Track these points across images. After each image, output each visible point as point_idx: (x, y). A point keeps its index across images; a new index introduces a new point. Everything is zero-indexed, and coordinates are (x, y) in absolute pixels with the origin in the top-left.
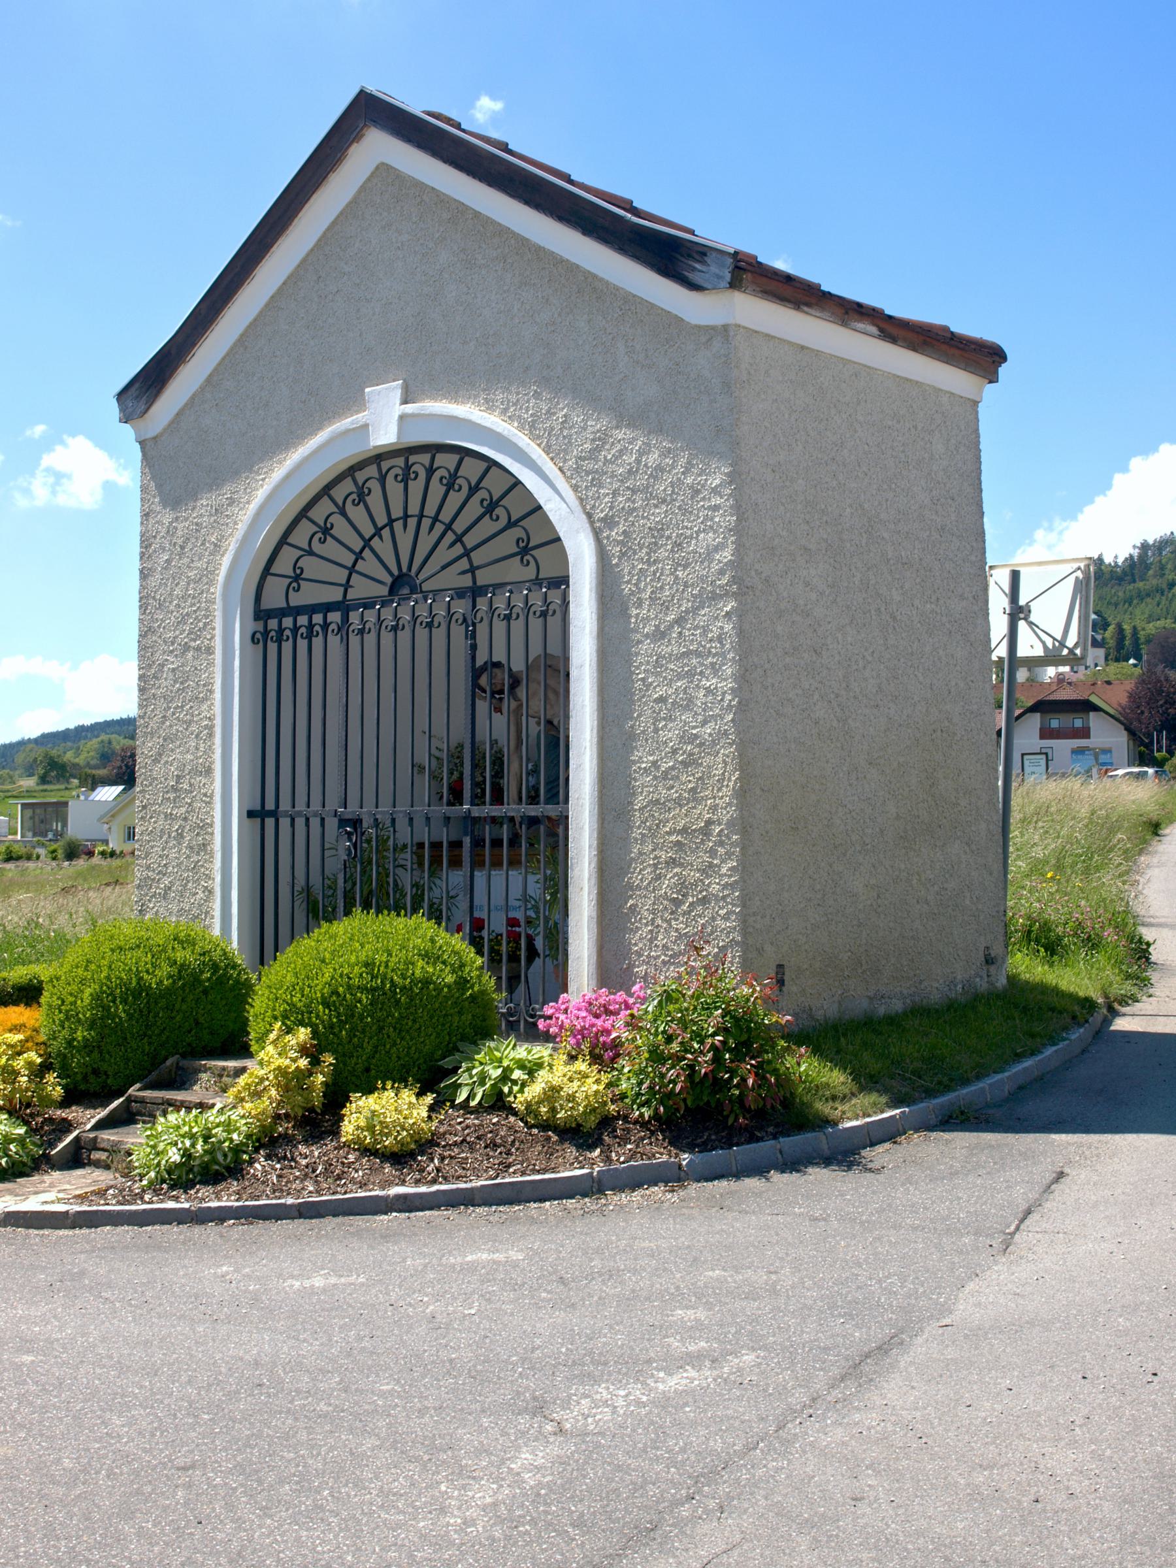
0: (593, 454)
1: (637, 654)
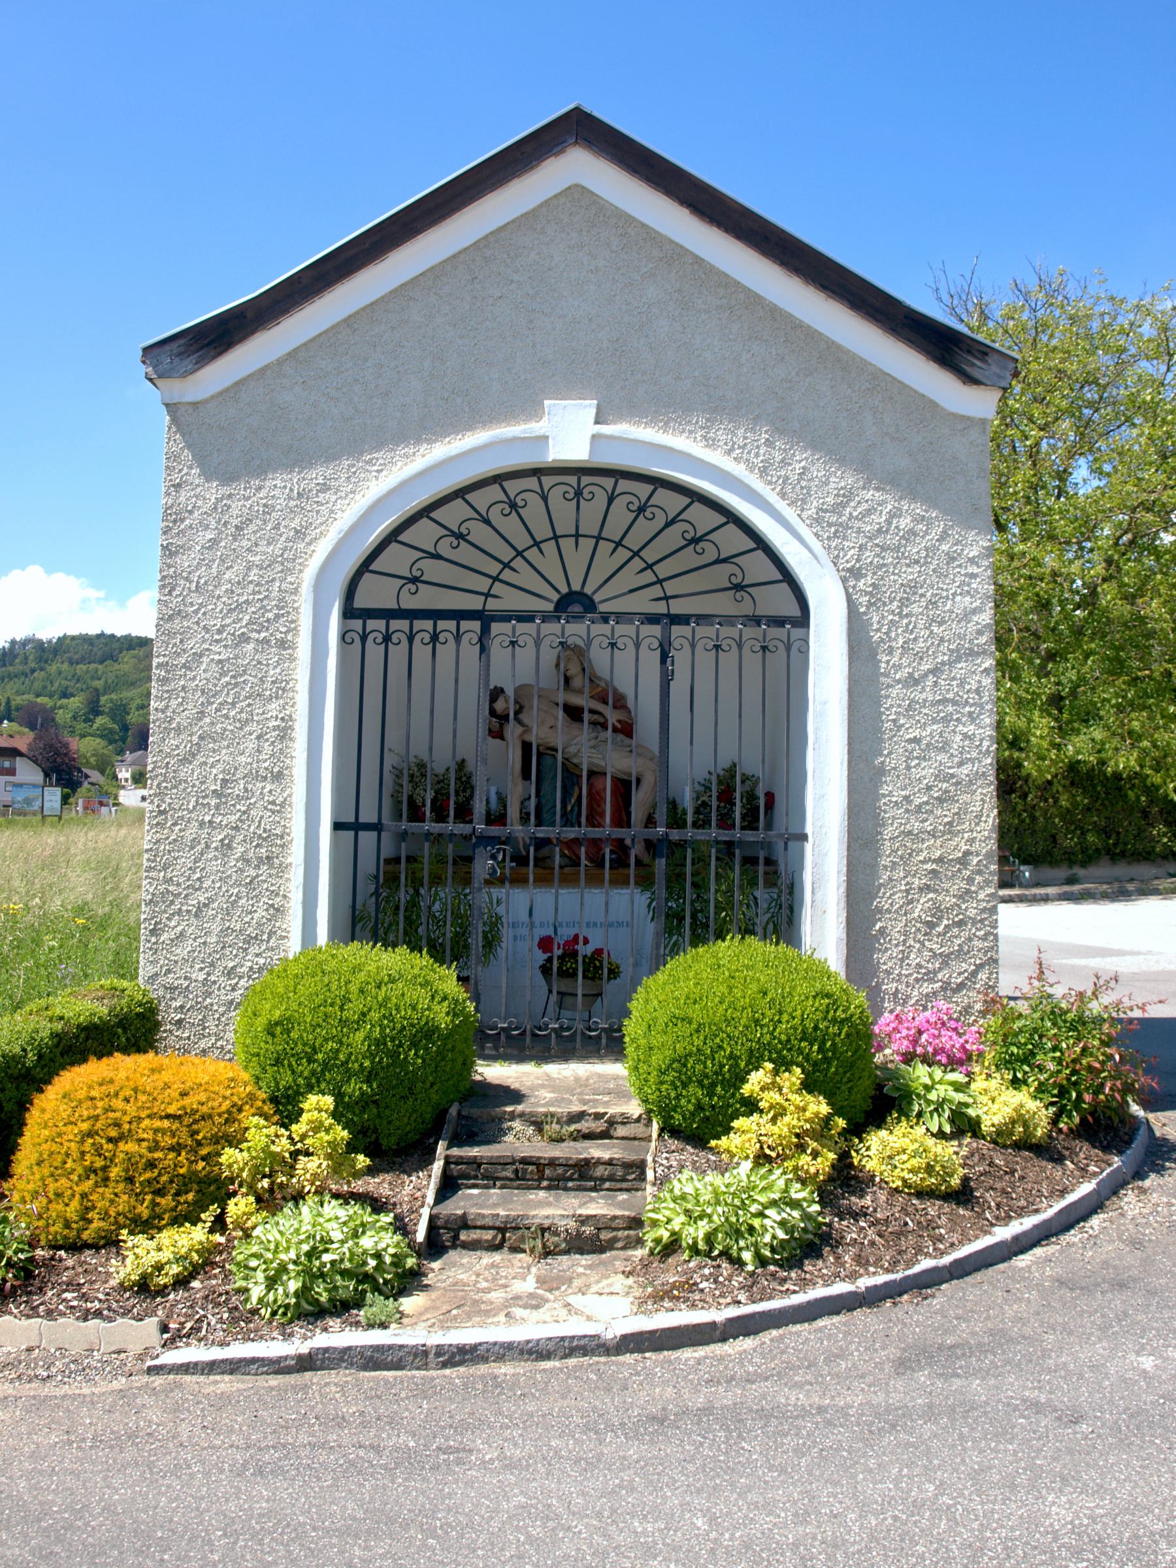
0: (838, 508)
1: (887, 697)
